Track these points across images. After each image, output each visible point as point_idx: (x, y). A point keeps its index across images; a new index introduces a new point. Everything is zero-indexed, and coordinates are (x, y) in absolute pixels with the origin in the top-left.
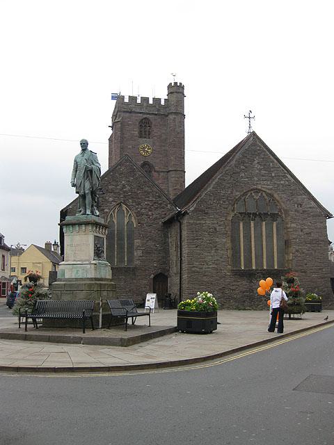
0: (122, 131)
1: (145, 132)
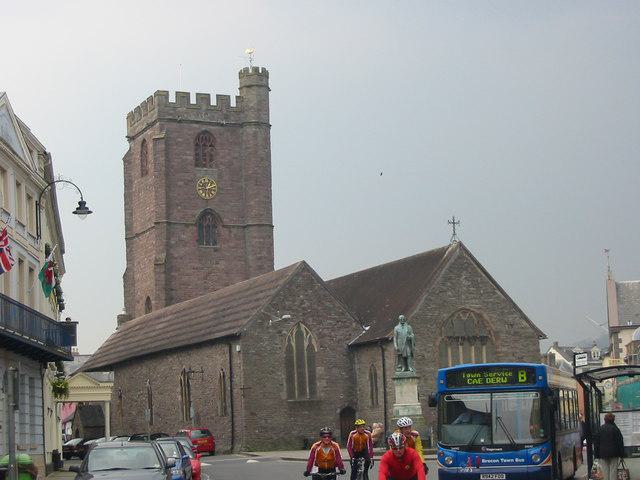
0: (167, 152)
1: (204, 155)
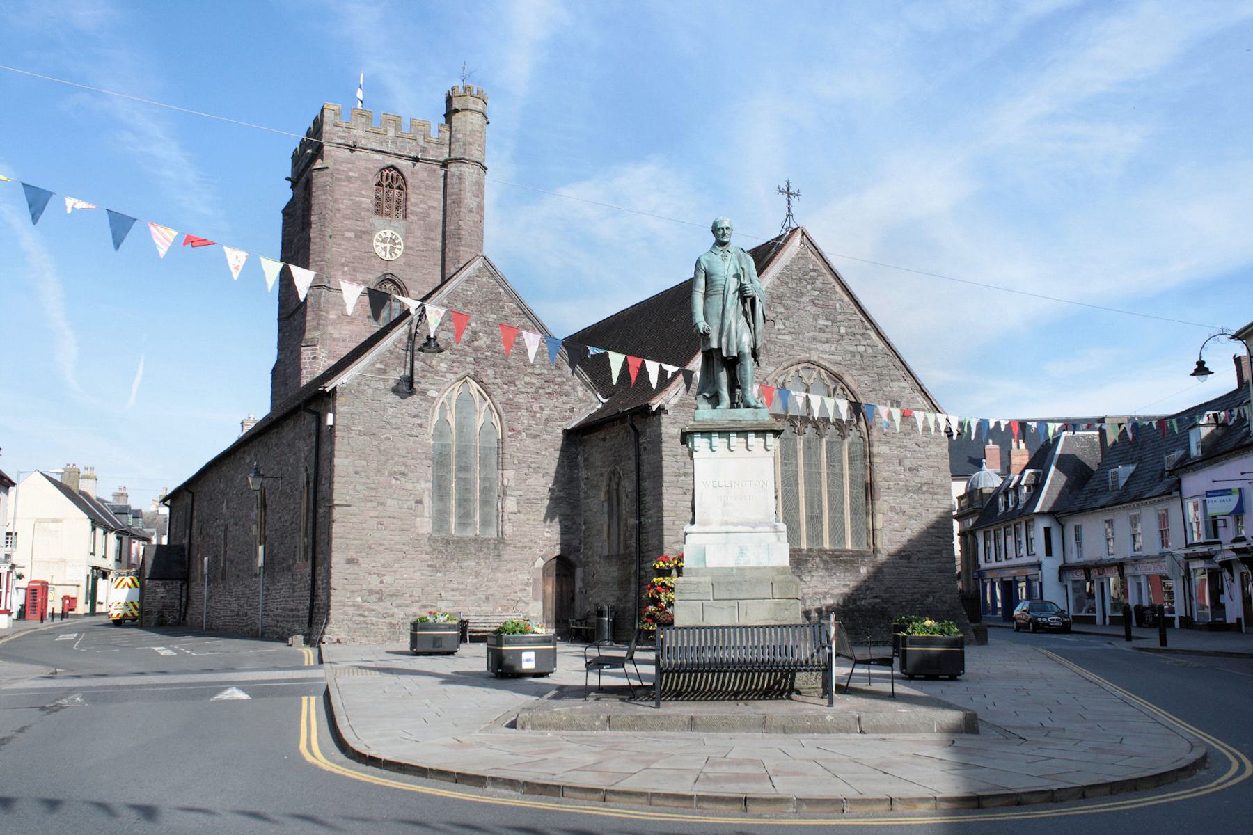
1: (388, 200)
